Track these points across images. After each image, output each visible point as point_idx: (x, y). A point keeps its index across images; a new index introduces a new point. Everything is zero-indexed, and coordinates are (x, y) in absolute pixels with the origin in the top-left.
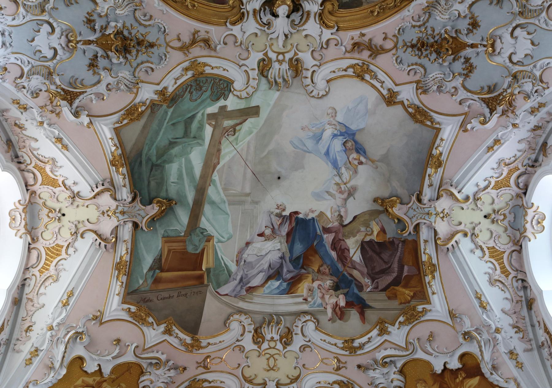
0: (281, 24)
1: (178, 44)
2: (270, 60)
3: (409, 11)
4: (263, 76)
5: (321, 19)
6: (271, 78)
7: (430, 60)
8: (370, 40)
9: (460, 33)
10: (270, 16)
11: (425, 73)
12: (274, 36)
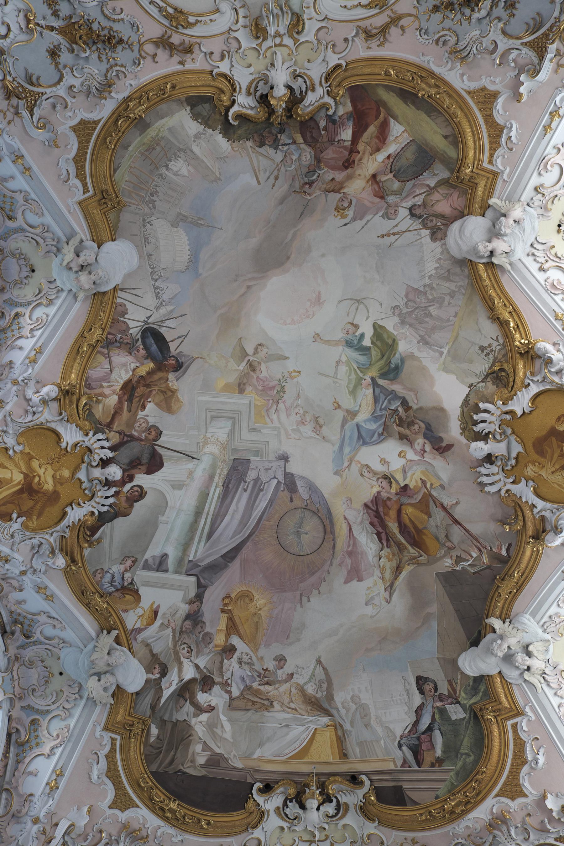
0: (280, 78)
1: (403, 22)
2: (291, 36)
3: (131, 85)
4: (297, 14)
5: (232, 85)
6: (287, 12)
7: (99, 23)
8: (171, 56)
9: (68, 48)
10: (295, 87)
11: (102, 7)
12: (287, 65)
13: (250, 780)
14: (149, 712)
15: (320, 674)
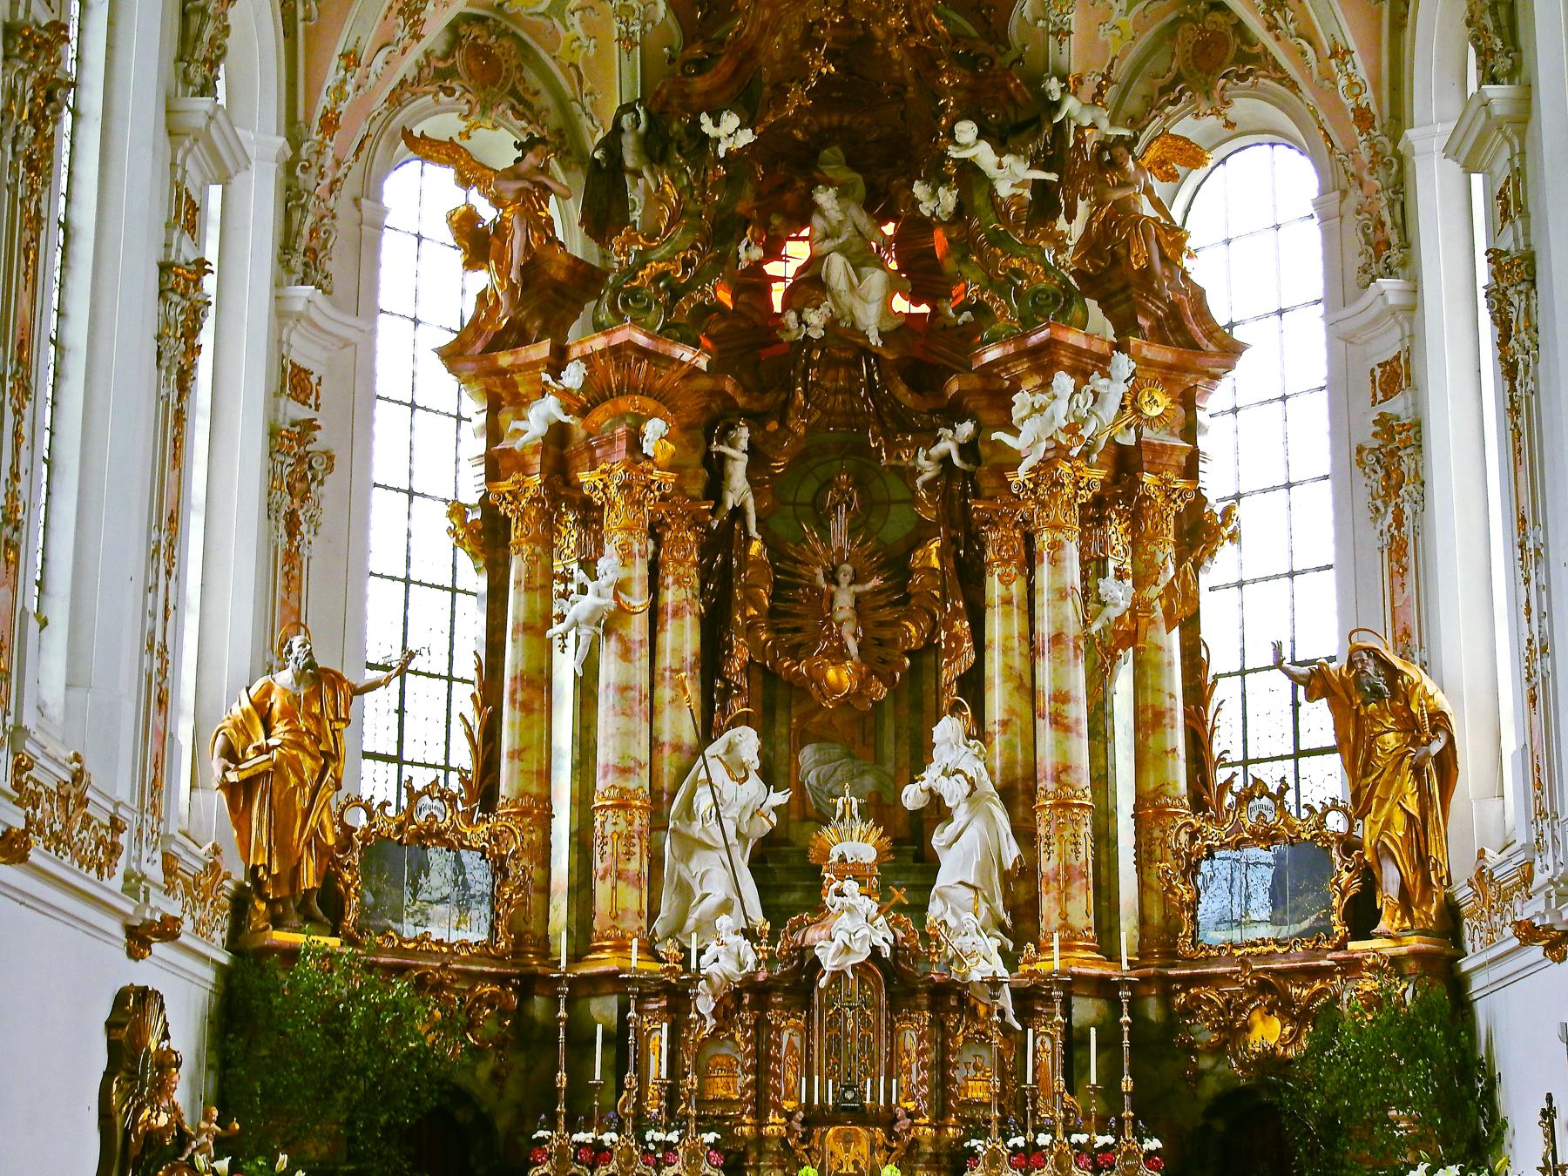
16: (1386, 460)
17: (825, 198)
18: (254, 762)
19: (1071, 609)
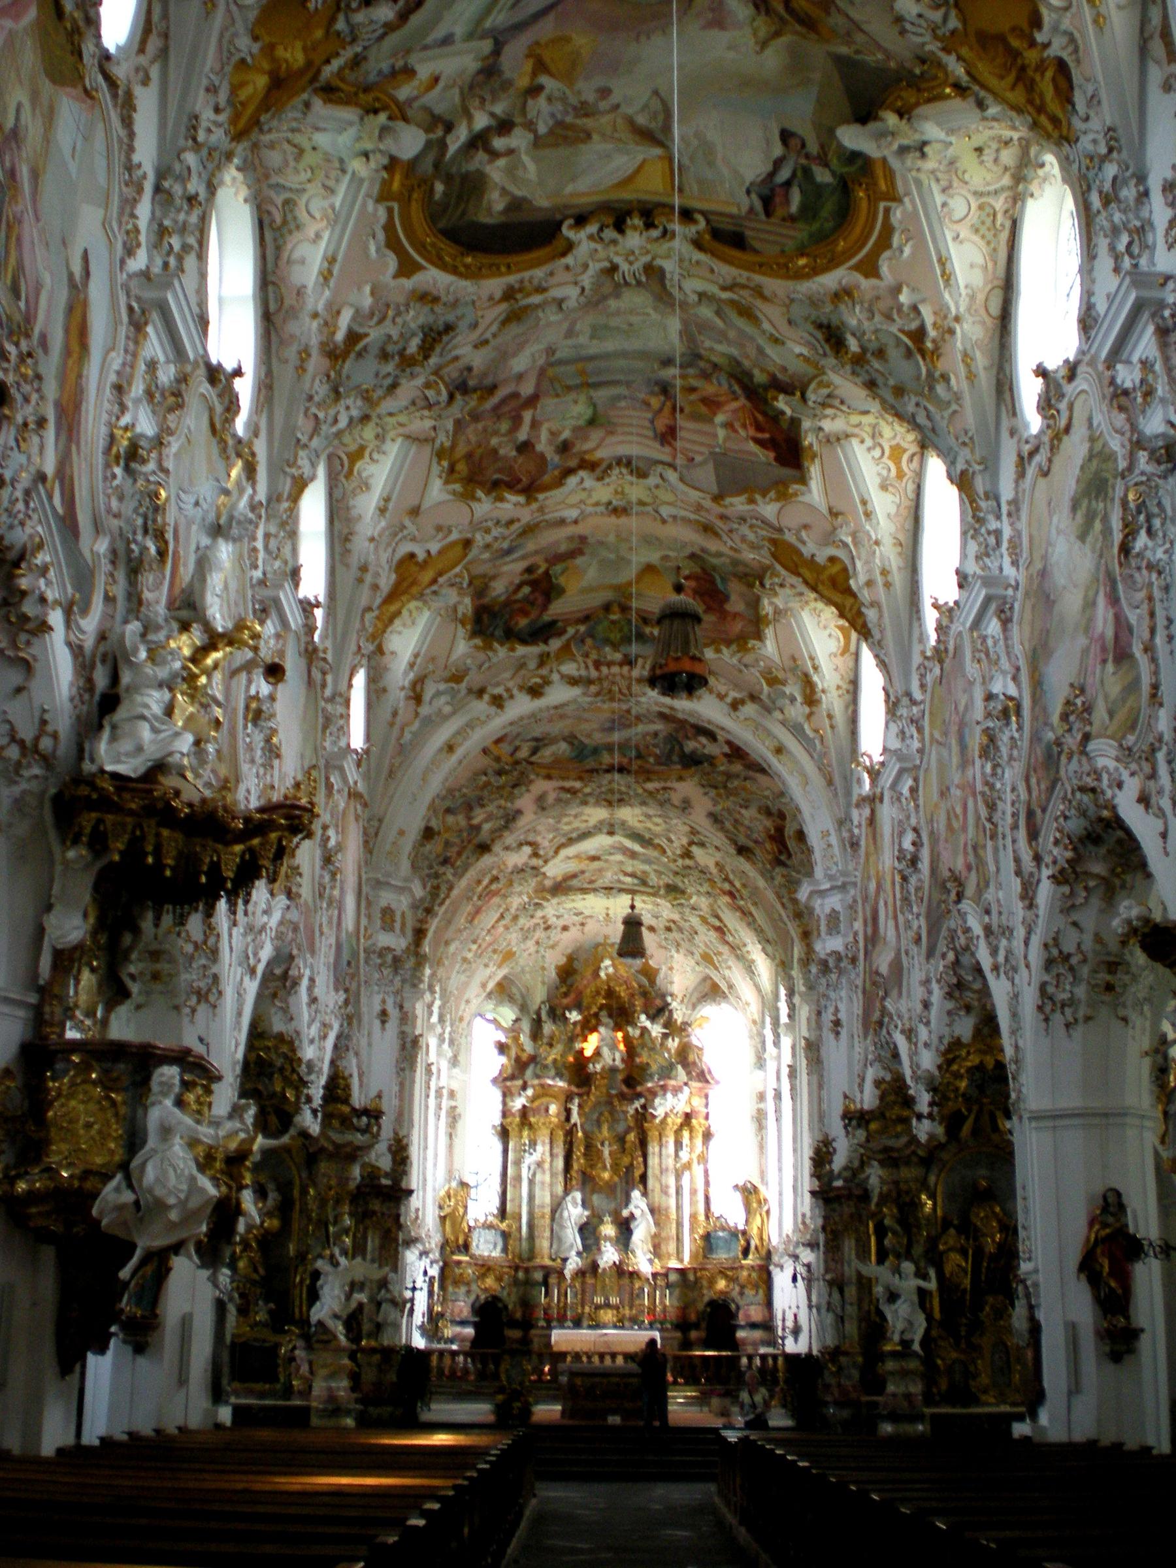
13: (558, 217)
14: (430, 170)
15: (656, 104)
16: (760, 1119)
17: (602, 1029)
18: (447, 1210)
19: (670, 1162)
